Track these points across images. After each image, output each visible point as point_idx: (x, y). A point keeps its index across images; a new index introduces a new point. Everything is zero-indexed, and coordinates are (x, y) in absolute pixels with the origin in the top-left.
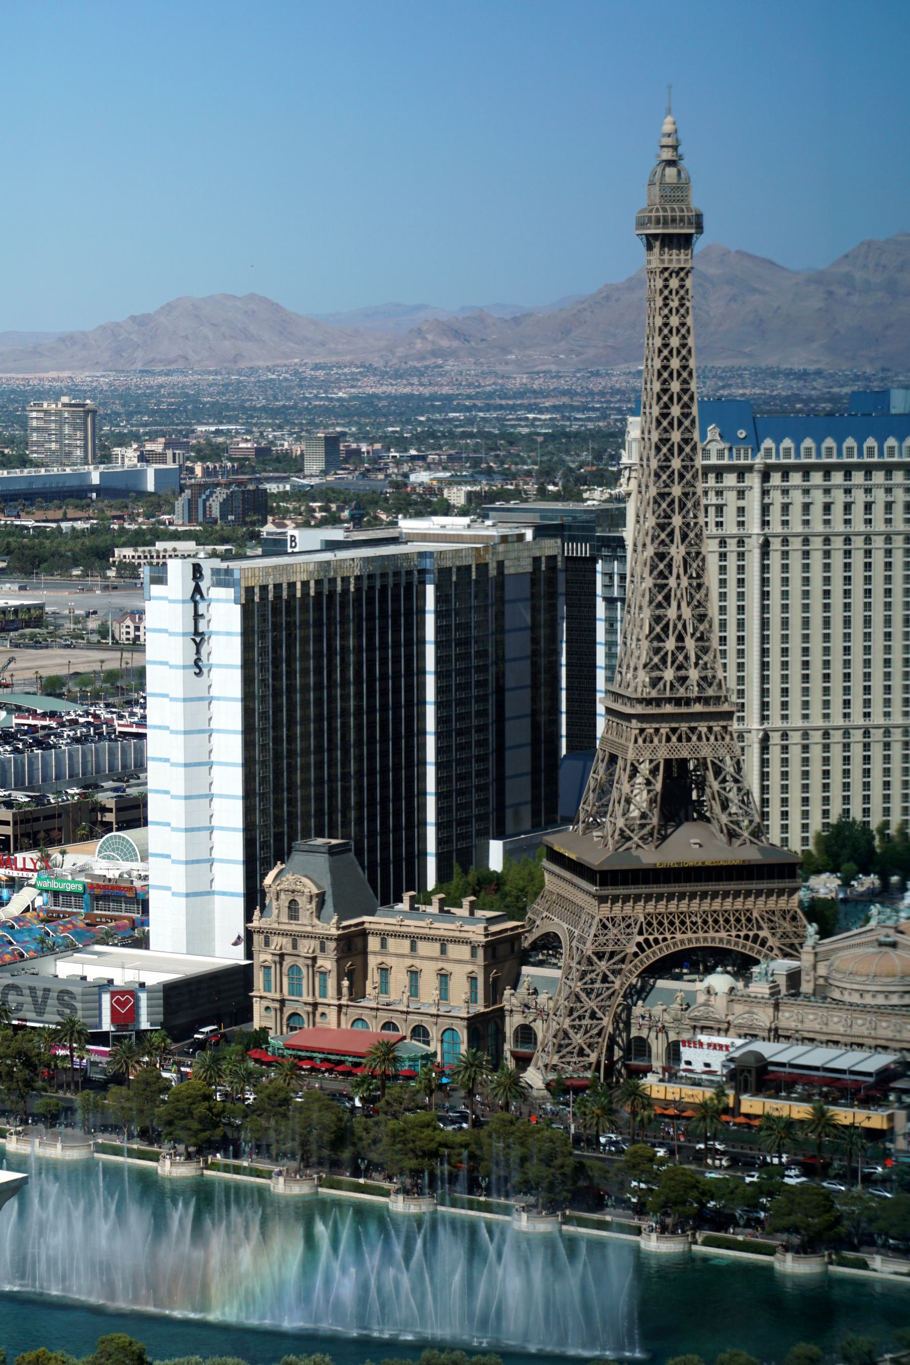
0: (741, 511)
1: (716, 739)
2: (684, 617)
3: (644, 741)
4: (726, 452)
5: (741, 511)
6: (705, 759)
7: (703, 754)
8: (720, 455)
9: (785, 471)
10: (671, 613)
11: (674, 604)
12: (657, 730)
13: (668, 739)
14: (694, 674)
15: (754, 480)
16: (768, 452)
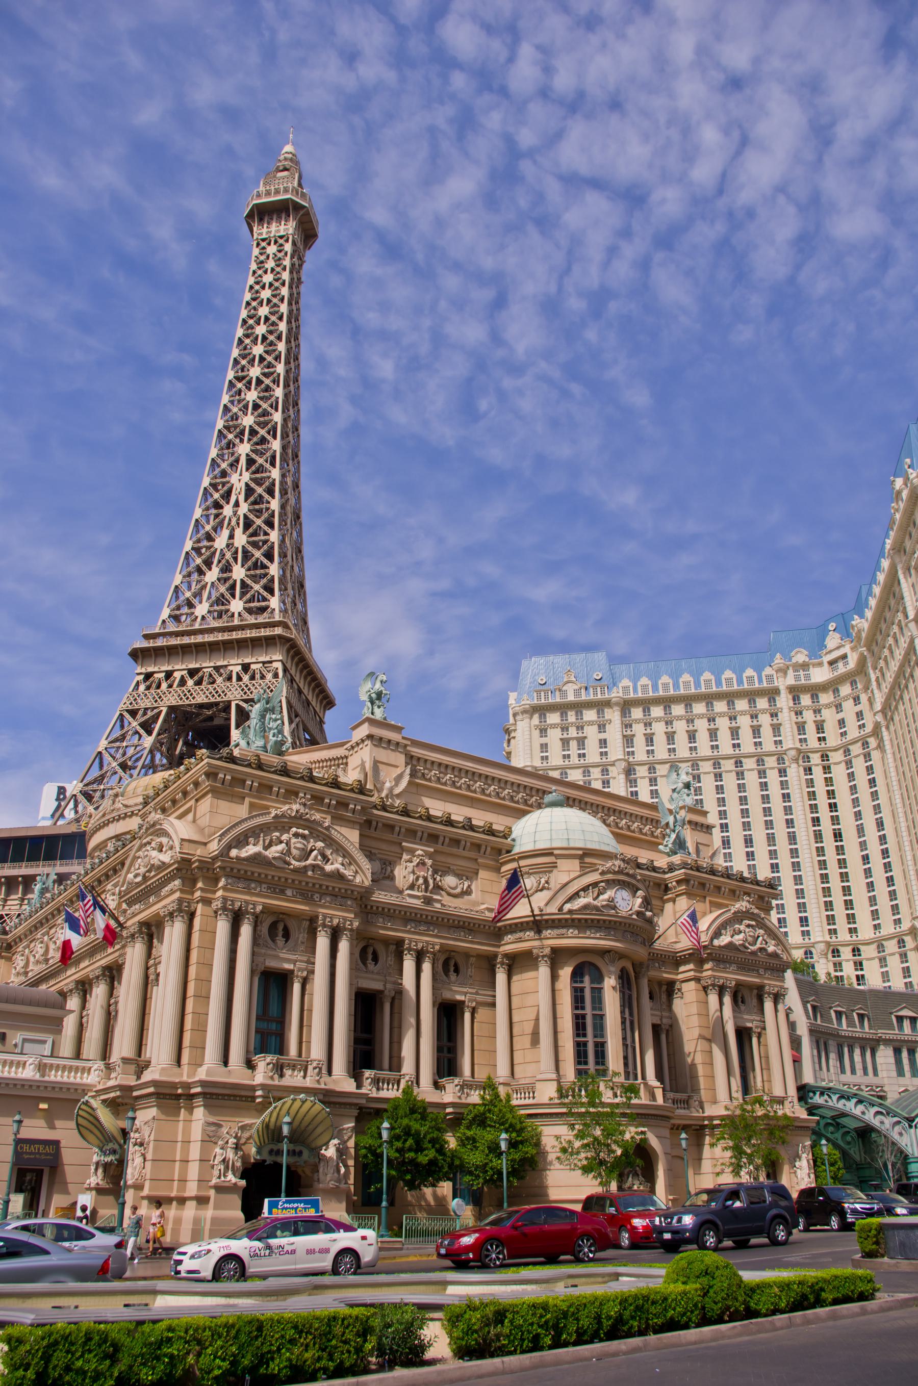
0: (603, 743)
1: (253, 678)
2: (236, 545)
3: (148, 688)
4: (583, 691)
5: (603, 743)
6: (230, 702)
7: (229, 696)
8: (577, 692)
9: (646, 704)
10: (220, 542)
11: (226, 533)
12: (169, 675)
13: (183, 682)
14: (236, 606)
15: (613, 715)
16: (626, 688)
